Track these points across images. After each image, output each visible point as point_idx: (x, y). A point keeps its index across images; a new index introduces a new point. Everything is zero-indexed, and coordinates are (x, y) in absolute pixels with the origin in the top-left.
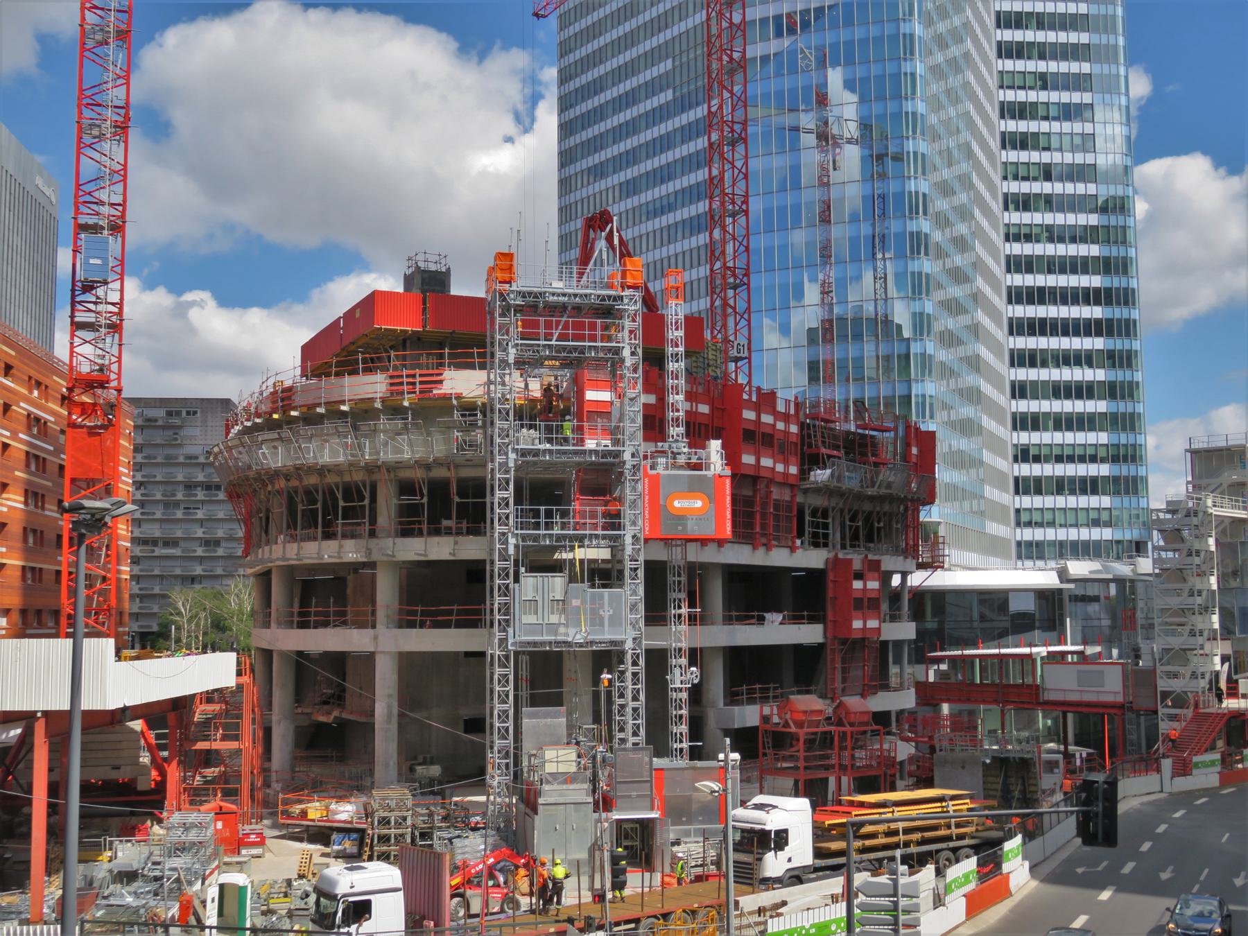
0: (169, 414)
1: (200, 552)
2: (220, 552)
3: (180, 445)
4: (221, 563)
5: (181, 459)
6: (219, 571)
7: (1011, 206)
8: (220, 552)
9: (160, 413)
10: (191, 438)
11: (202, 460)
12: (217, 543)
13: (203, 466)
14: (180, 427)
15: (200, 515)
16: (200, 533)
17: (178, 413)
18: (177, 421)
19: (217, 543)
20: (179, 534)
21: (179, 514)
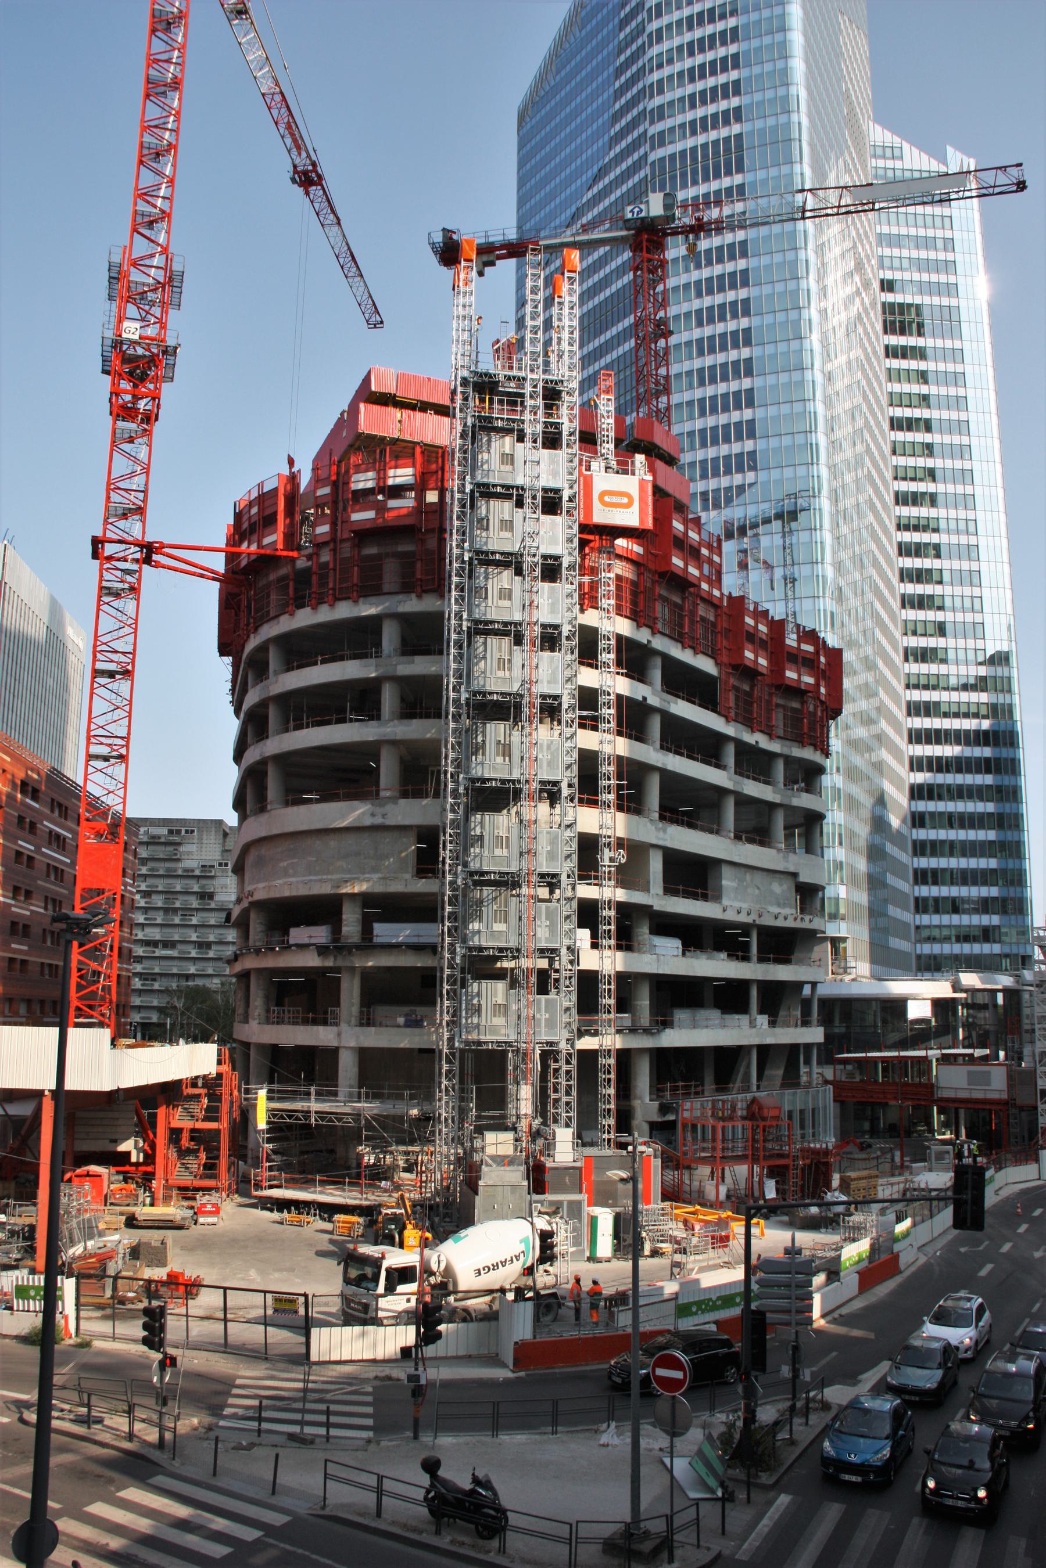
0: (171, 832)
1: (194, 954)
2: (211, 954)
3: (178, 860)
4: (211, 964)
5: (180, 872)
6: (210, 971)
7: (911, 658)
8: (211, 954)
9: (163, 831)
10: (189, 853)
11: (197, 873)
12: (208, 945)
13: (198, 877)
14: (179, 844)
15: (194, 921)
16: (194, 938)
17: (179, 832)
18: (176, 839)
19: (208, 945)
20: (176, 938)
21: (177, 920)
